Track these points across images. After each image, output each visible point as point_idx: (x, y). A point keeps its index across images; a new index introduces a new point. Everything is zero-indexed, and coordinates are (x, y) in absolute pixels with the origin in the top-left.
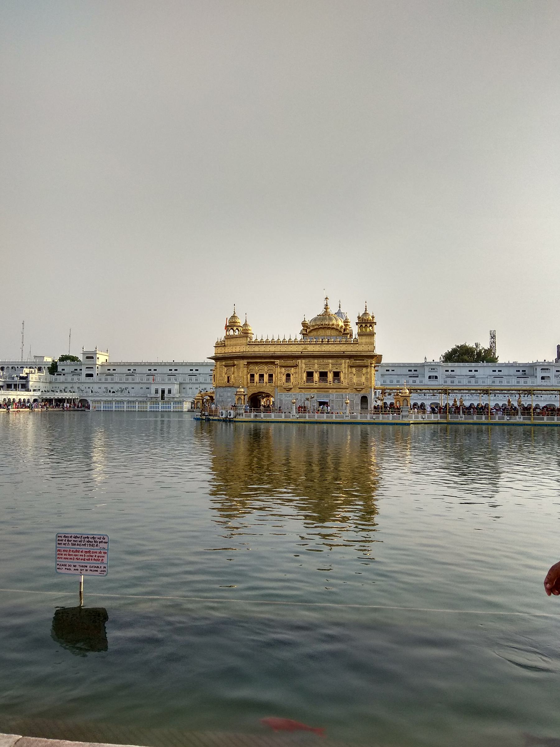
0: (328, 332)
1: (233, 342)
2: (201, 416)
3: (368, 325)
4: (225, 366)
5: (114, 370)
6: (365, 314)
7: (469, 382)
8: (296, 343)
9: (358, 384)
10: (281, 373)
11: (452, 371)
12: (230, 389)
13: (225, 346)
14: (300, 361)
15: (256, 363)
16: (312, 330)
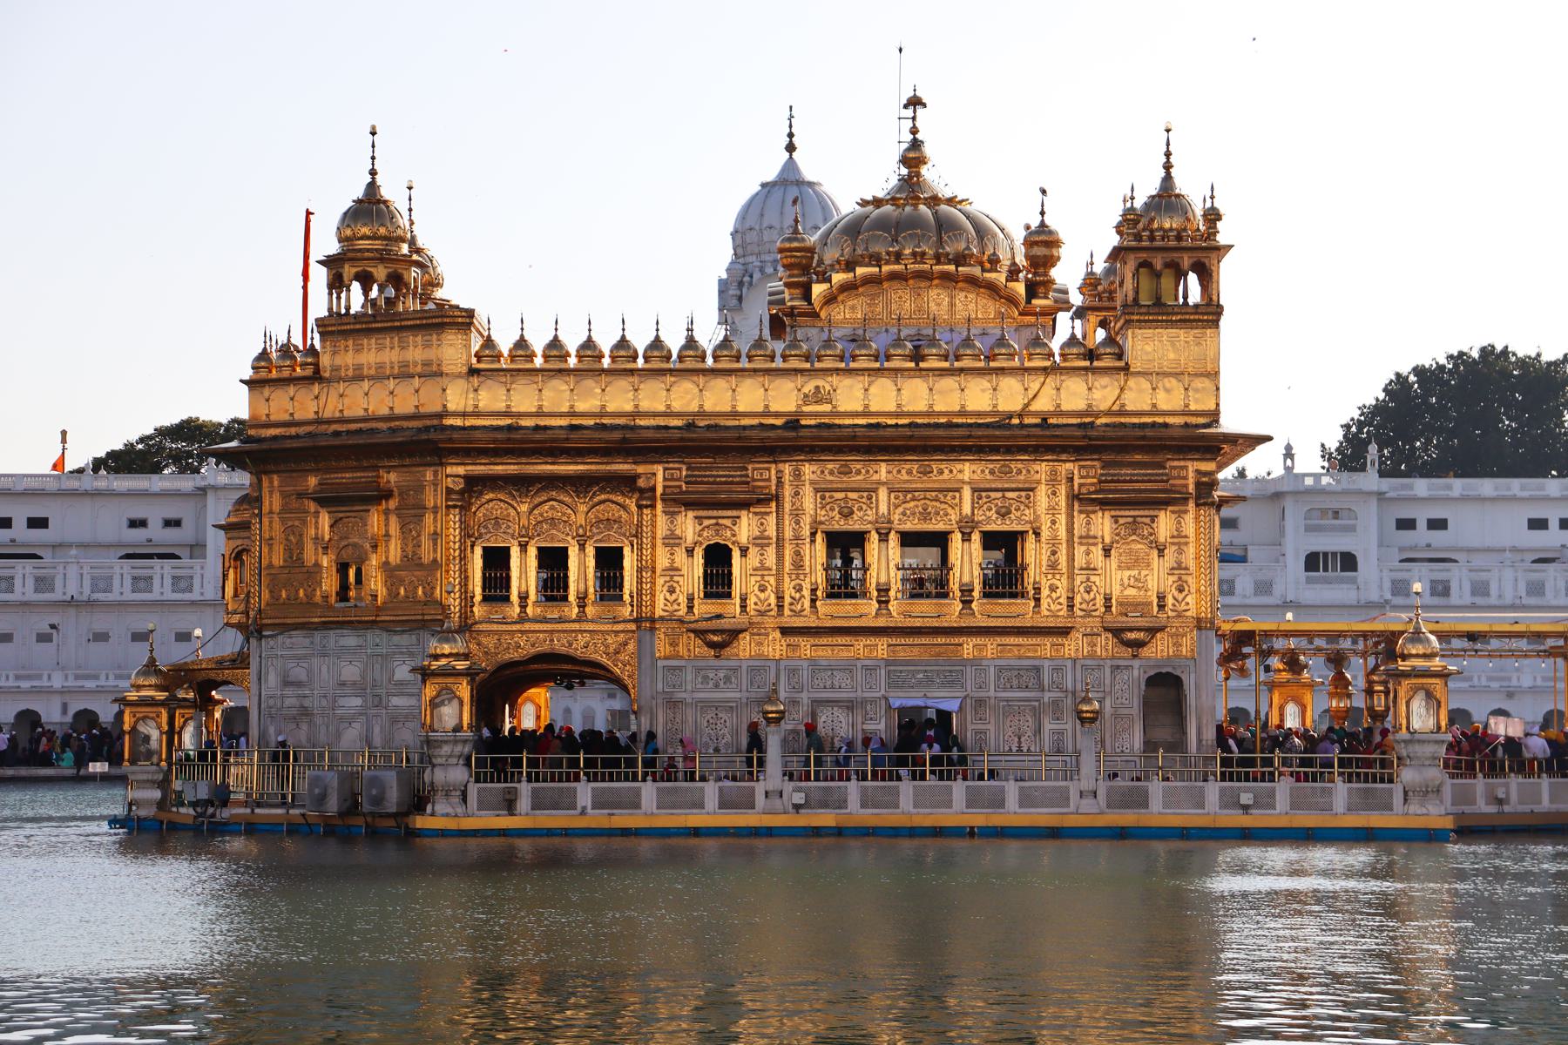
0: (937, 301)
1: (371, 354)
2: (161, 804)
3: (1186, 262)
4: (323, 502)
5: (38, 523)
6: (1167, 198)
7: (1536, 589)
8: (689, 363)
9: (1128, 606)
10: (672, 540)
11: (1438, 524)
12: (350, 640)
13: (316, 377)
14: (787, 469)
15: (521, 484)
16: (846, 288)
